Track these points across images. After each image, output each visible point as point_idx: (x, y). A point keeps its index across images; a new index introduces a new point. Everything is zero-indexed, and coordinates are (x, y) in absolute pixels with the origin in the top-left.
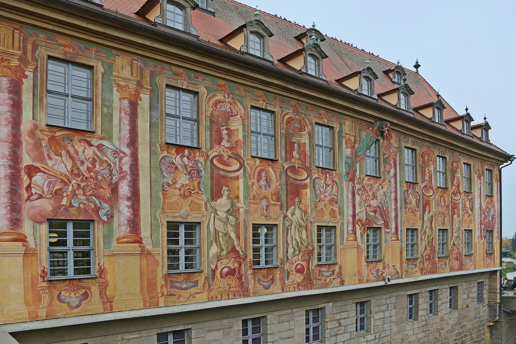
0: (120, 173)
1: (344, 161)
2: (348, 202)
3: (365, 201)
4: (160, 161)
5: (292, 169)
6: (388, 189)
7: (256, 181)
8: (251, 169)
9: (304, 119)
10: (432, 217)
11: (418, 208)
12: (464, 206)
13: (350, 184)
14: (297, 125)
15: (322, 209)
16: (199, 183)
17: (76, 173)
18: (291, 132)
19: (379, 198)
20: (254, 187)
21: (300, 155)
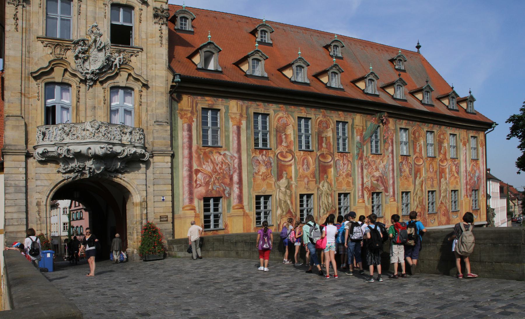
2: (358, 175)
3: (370, 173)
5: (323, 155)
7: (301, 166)
9: (329, 120)
10: (422, 181)
11: (411, 175)
12: (451, 171)
13: (360, 162)
14: (325, 125)
16: (271, 171)
17: (215, 171)
18: (321, 130)
19: (380, 170)
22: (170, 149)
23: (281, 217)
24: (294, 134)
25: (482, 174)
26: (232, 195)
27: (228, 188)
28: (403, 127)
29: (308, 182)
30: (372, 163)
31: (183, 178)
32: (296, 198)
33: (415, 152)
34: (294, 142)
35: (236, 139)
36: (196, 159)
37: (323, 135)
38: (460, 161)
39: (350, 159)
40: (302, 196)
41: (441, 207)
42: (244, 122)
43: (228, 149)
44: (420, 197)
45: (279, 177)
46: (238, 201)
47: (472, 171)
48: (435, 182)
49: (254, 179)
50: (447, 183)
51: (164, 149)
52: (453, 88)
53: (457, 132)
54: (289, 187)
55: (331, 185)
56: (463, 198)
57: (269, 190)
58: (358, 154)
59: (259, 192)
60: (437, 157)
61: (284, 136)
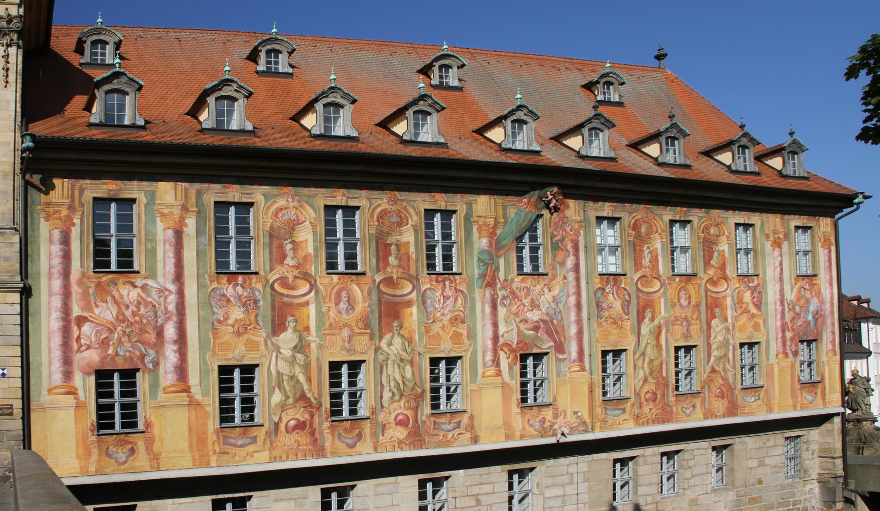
0: (166, 314)
1: (476, 259)
2: (483, 318)
3: (516, 314)
4: (210, 295)
5: (389, 281)
6: (561, 291)
7: (332, 305)
8: (326, 290)
9: (405, 208)
10: (659, 327)
12: (739, 301)
14: (395, 219)
15: (438, 333)
16: (256, 316)
17: (121, 318)
18: (385, 229)
19: (544, 307)
20: (331, 313)
21: (400, 260)
22: (18, 278)
23: (283, 407)
24: (314, 241)
25: (828, 306)
26: (161, 366)
27: (151, 352)
28: (605, 215)
29: (350, 338)
31: (50, 333)
32: (320, 370)
33: (638, 266)
34: (316, 256)
35: (171, 254)
36: (79, 297)
37: (391, 240)
38: (764, 280)
39: (463, 287)
40: (335, 366)
41: (711, 380)
42: (191, 223)
43: (154, 276)
44: (651, 361)
45: (278, 327)
46: (176, 377)
47: (798, 300)
48: (695, 328)
49: (213, 334)
50: (728, 329)
51: (7, 278)
52: (742, 127)
53: (755, 218)
54: (301, 347)
55: (410, 341)
56: (772, 359)
57: (250, 356)
58: (483, 276)
59: (229, 360)
60: (701, 274)
61: (289, 247)
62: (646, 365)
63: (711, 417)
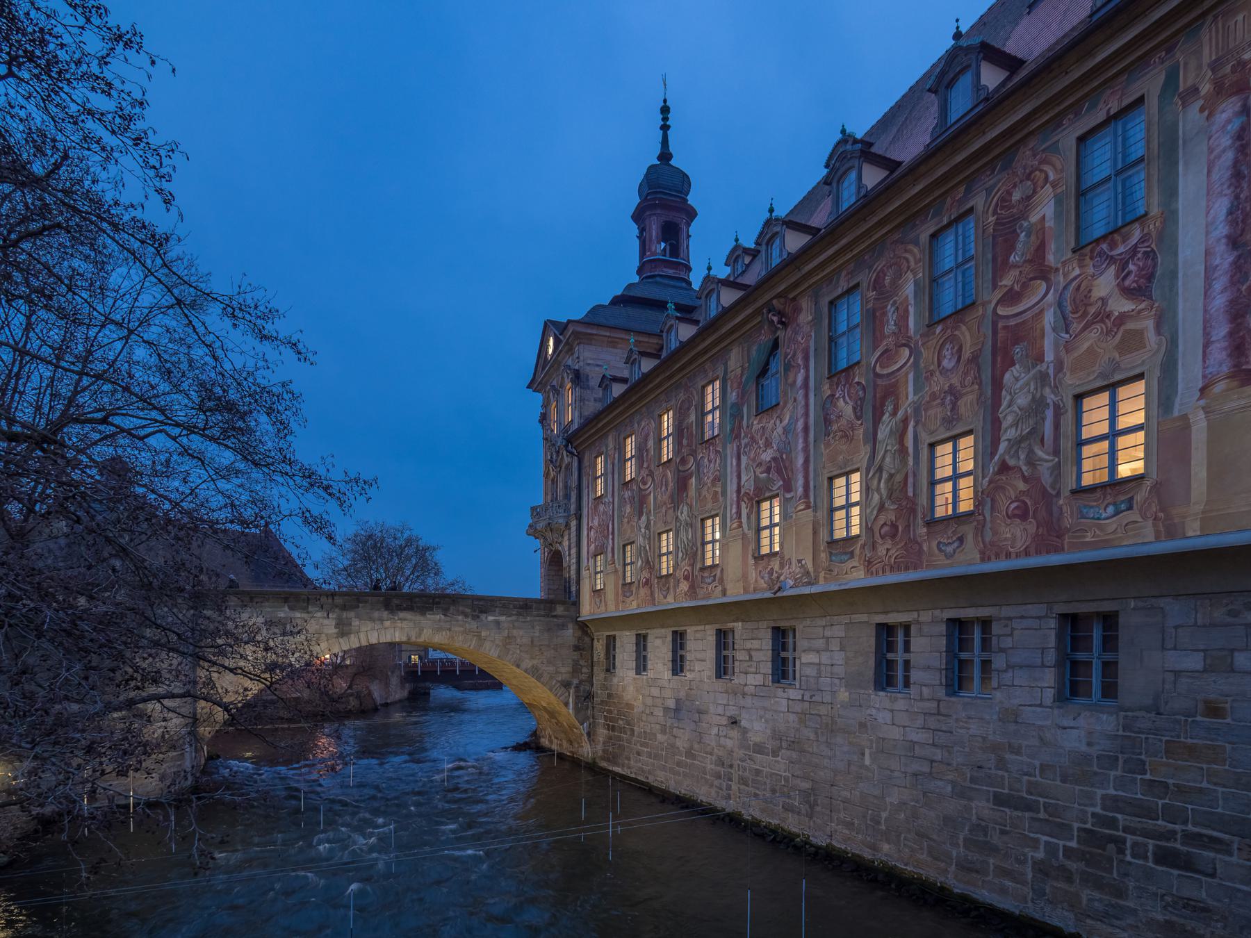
3: (754, 460)
10: (905, 421)
30: (758, 437)
44: (891, 476)
50: (1043, 378)
55: (691, 507)
58: (732, 430)
62: (882, 485)
63: (997, 556)
